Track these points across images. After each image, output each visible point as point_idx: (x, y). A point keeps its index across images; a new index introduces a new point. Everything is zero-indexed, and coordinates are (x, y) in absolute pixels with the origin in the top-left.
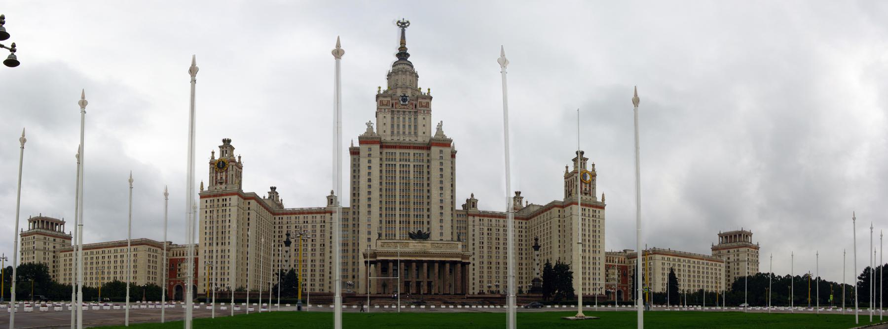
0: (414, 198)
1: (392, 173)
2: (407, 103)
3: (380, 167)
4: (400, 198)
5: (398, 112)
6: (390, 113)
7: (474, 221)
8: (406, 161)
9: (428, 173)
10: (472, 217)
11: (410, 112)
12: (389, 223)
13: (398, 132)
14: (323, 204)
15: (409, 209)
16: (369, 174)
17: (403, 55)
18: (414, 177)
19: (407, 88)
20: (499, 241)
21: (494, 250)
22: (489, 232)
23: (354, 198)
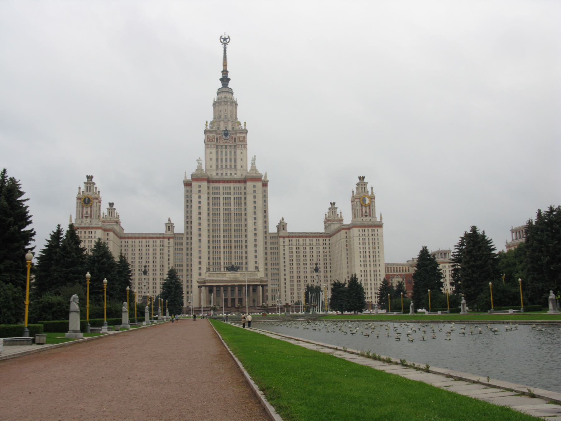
0: (235, 226)
1: (217, 205)
2: (228, 137)
3: (208, 200)
4: (224, 226)
5: (222, 146)
6: (215, 149)
7: (284, 242)
8: (228, 194)
9: (245, 203)
10: (283, 238)
11: (230, 146)
12: (215, 248)
13: (222, 166)
14: (162, 230)
15: (231, 235)
16: (200, 208)
17: (225, 80)
18: (234, 208)
19: (228, 121)
20: (307, 258)
21: (302, 266)
22: (298, 250)
23: (188, 225)
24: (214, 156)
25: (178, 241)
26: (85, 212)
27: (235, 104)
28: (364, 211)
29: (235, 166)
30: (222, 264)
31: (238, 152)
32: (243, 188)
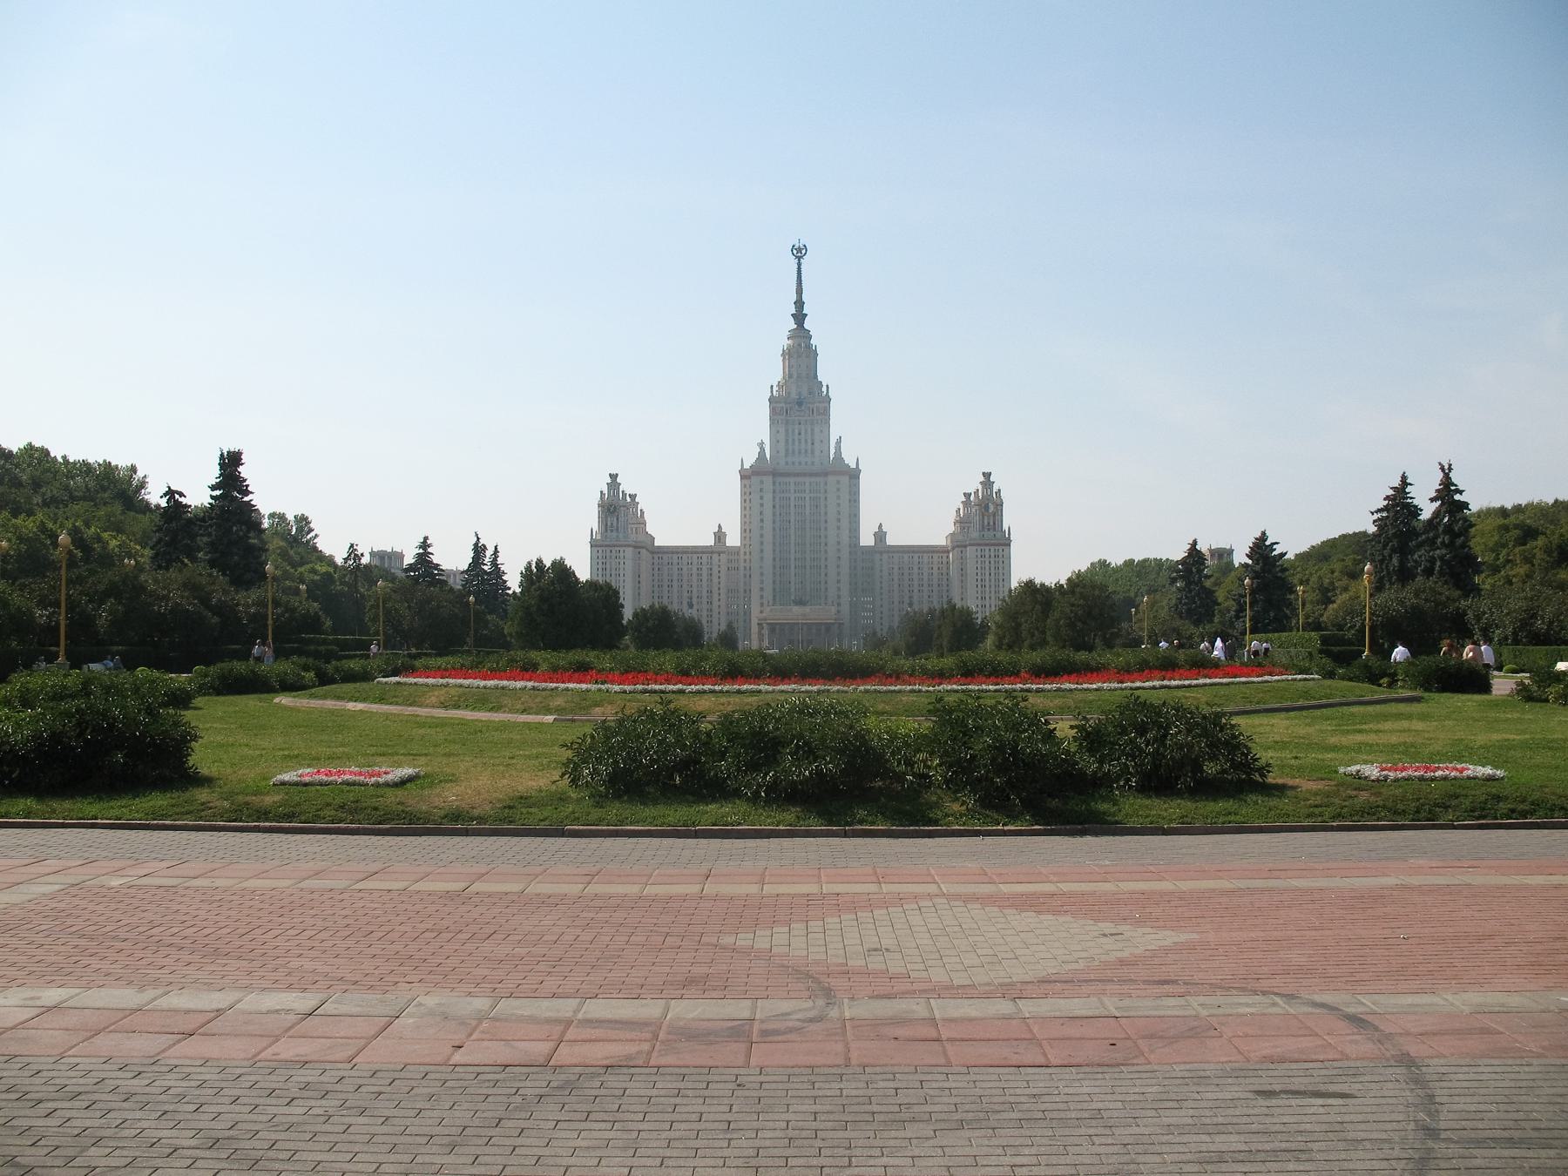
2: (803, 408)
11: (806, 421)
14: (709, 541)
17: (799, 317)
24: (782, 437)
25: (733, 557)
26: (609, 524)
27: (812, 354)
28: (986, 523)
29: (813, 452)
30: (792, 590)
31: (817, 429)
32: (822, 485)
